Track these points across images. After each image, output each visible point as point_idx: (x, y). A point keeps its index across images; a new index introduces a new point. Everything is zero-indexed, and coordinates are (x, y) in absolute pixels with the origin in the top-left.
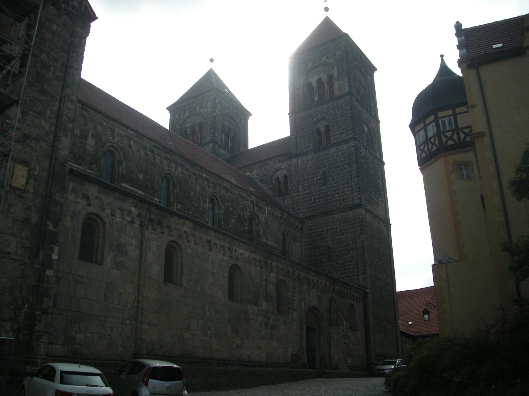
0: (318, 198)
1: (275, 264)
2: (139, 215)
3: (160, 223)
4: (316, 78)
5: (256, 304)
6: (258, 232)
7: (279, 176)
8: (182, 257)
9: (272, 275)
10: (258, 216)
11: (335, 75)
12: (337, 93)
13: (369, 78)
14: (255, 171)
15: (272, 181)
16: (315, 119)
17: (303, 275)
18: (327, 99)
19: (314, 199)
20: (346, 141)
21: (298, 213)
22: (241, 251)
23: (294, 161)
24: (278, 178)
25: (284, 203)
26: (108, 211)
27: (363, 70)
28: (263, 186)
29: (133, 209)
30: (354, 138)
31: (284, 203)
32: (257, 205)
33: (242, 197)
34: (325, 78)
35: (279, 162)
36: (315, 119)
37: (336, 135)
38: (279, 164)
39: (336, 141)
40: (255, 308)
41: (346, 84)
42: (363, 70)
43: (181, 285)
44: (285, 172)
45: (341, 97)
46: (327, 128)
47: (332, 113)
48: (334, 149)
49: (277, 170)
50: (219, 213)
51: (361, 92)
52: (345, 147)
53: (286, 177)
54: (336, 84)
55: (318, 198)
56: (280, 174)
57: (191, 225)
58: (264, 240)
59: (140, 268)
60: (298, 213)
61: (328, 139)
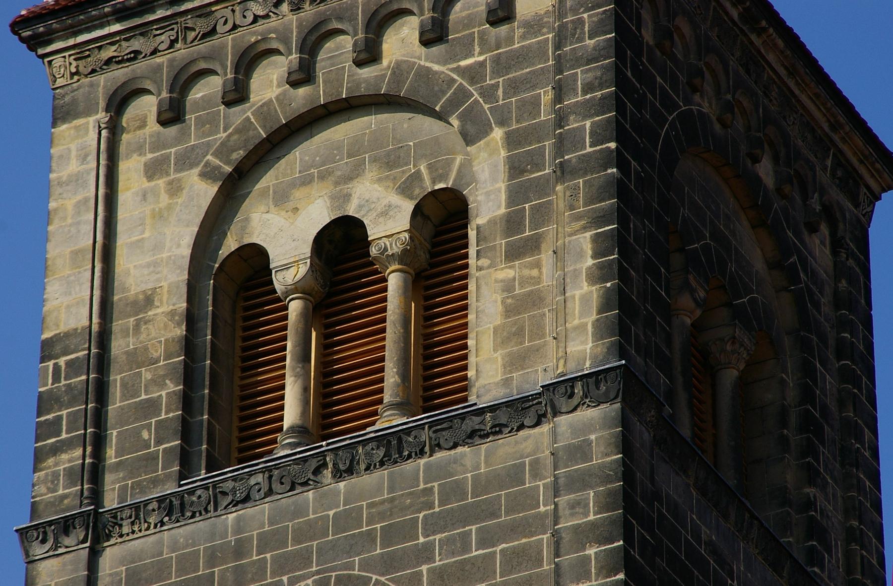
4: (317, 214)
11: (488, 204)
12: (488, 373)
13: (819, 249)
18: (389, 420)
27: (765, 170)
34: (389, 222)
42: (765, 170)
45: (524, 411)
47: (425, 554)
51: (729, 376)
54: (488, 288)
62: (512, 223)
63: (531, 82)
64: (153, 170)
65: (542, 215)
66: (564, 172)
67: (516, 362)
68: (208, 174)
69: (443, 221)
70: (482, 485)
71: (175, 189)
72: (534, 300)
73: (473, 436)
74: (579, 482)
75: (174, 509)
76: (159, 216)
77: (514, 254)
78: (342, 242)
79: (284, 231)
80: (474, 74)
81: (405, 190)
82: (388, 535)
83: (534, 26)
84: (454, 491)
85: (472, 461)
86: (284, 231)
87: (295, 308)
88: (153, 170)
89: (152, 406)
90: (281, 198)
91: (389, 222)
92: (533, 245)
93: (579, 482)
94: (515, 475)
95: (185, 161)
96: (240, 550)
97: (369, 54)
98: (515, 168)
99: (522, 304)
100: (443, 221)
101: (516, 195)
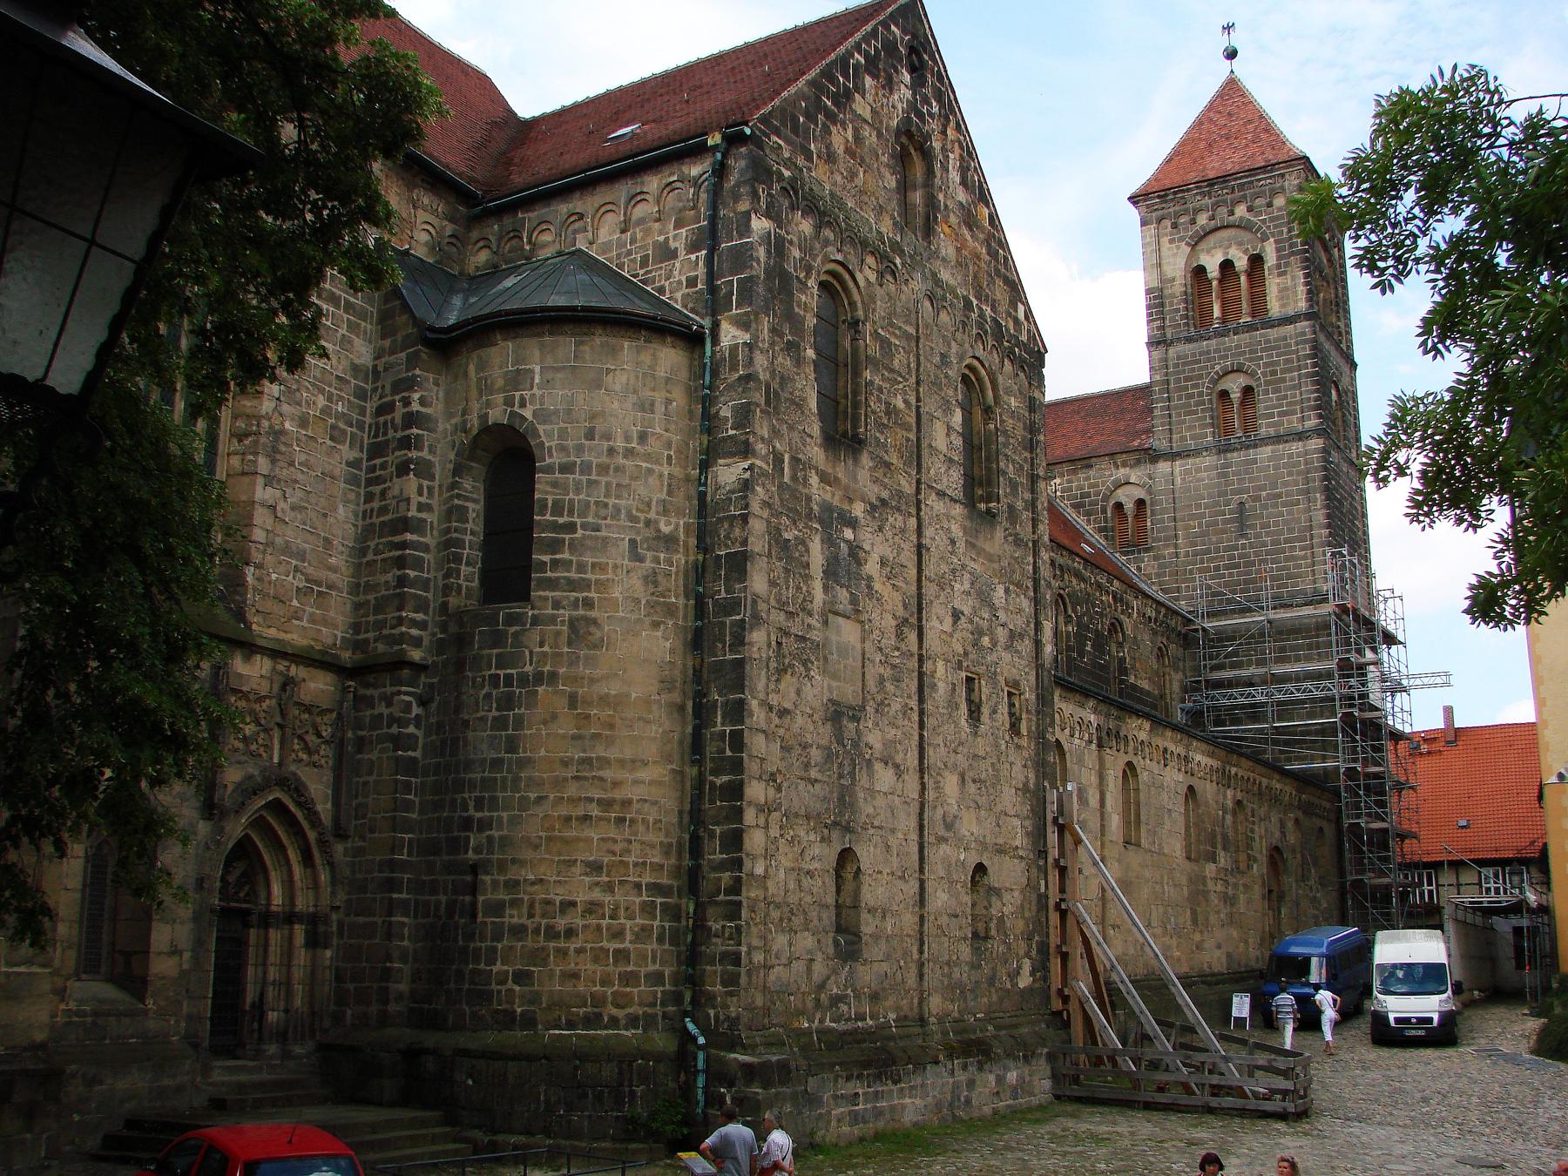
0: (1227, 567)
1: (1233, 770)
2: (1099, 728)
3: (1117, 736)
4: (1219, 258)
5: (1213, 858)
6: (1122, 660)
7: (1123, 500)
8: (1137, 790)
9: (1229, 793)
10: (1121, 625)
11: (1271, 258)
12: (1275, 308)
14: (1058, 481)
15: (1104, 511)
16: (1217, 368)
17: (1265, 781)
19: (1217, 568)
20: (1301, 436)
21: (1177, 599)
22: (1198, 757)
23: (1163, 467)
24: (1119, 506)
25: (1139, 569)
26: (1067, 731)
28: (1080, 521)
29: (1092, 718)
30: (1319, 432)
31: (1139, 569)
32: (1121, 600)
33: (1099, 586)
34: (1241, 263)
35: (1124, 465)
36: (1217, 368)
37: (1272, 416)
38: (1122, 471)
39: (1272, 431)
40: (1212, 866)
41: (1301, 290)
43: (1138, 845)
44: (1140, 493)
46: (1248, 391)
48: (1267, 451)
49: (1119, 485)
50: (1068, 633)
52: (1296, 447)
53: (1140, 503)
54: (1273, 285)
55: (1227, 567)
56: (1127, 497)
57: (1147, 725)
58: (1132, 679)
59: (1102, 826)
60: (1177, 599)
61: (1249, 425)
62: (1278, 266)
63: (1280, 225)
64: (1171, 241)
65: (1287, 265)
66: (1293, 254)
67: (1283, 306)
68: (1188, 244)
69: (1256, 261)
70: (1276, 340)
71: (1178, 248)
72: (1286, 289)
73: (1273, 327)
74: (1305, 342)
75: (1189, 340)
76: (1175, 255)
77: (1280, 275)
78: (1227, 266)
79: (1212, 264)
80: (1263, 221)
81: (1246, 251)
82: (1251, 352)
83: (1280, 209)
84: (1267, 341)
85: (1273, 333)
86: (1212, 264)
87: (1215, 283)
88: (1171, 241)
89: (1178, 310)
90: (1208, 251)
91: (1241, 263)
92: (1284, 273)
93: (1305, 342)
94: (1285, 338)
95: (1181, 239)
96: (1208, 352)
97: (1232, 213)
98: (1278, 250)
99: (1283, 290)
100: (1256, 261)
101: (1279, 258)
